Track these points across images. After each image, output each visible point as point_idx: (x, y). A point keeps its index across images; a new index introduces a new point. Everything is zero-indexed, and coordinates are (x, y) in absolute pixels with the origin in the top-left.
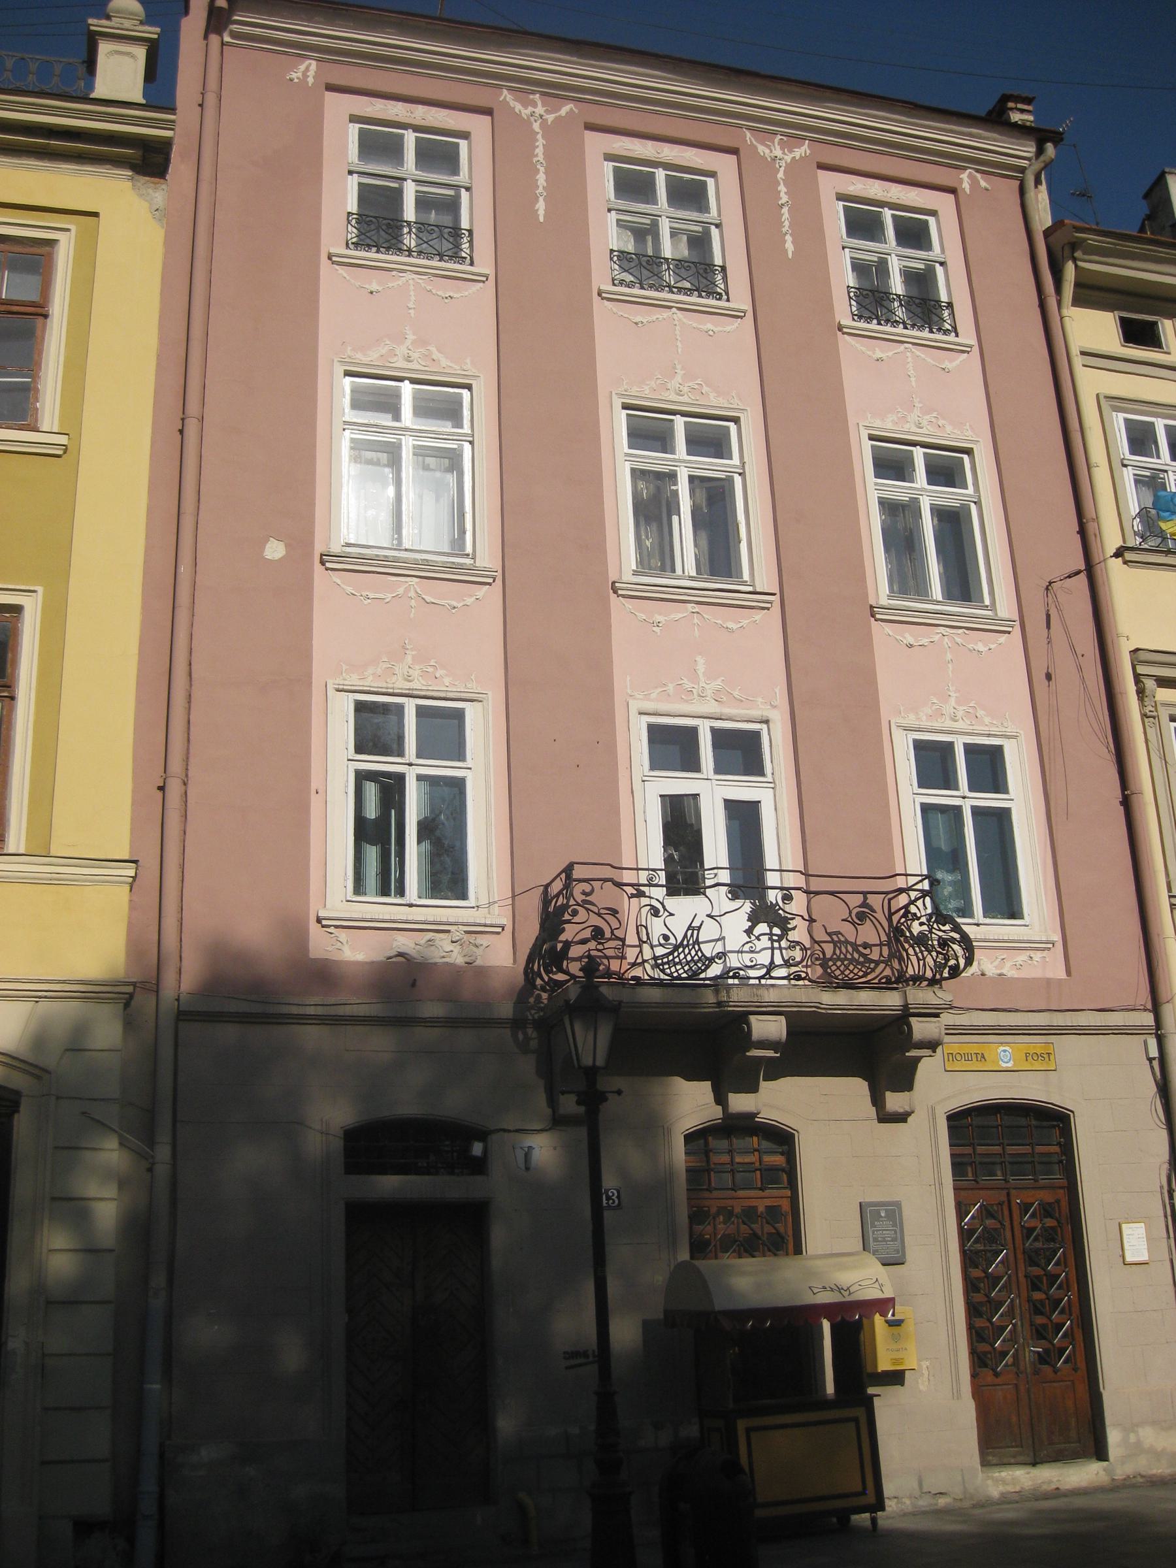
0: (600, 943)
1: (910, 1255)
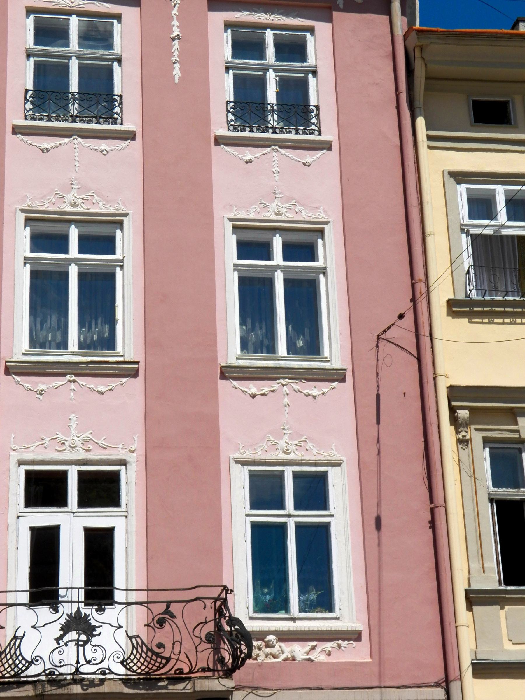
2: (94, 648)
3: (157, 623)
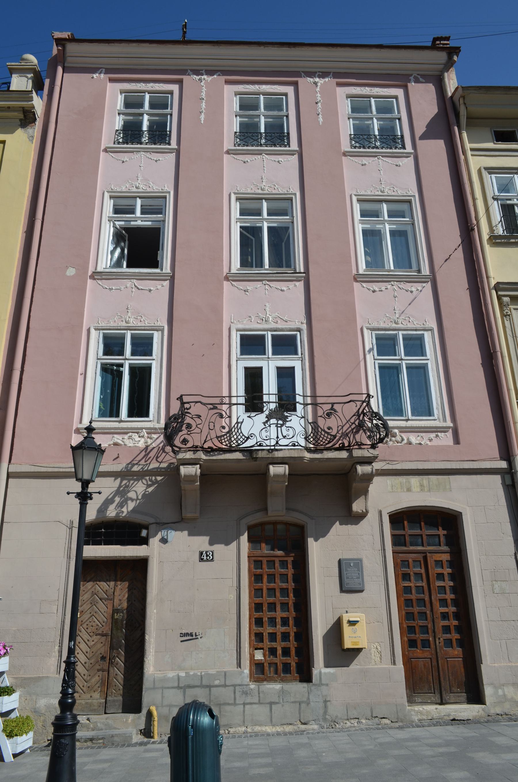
0: (189, 431)
1: (367, 586)
2: (288, 428)
3: (327, 415)
